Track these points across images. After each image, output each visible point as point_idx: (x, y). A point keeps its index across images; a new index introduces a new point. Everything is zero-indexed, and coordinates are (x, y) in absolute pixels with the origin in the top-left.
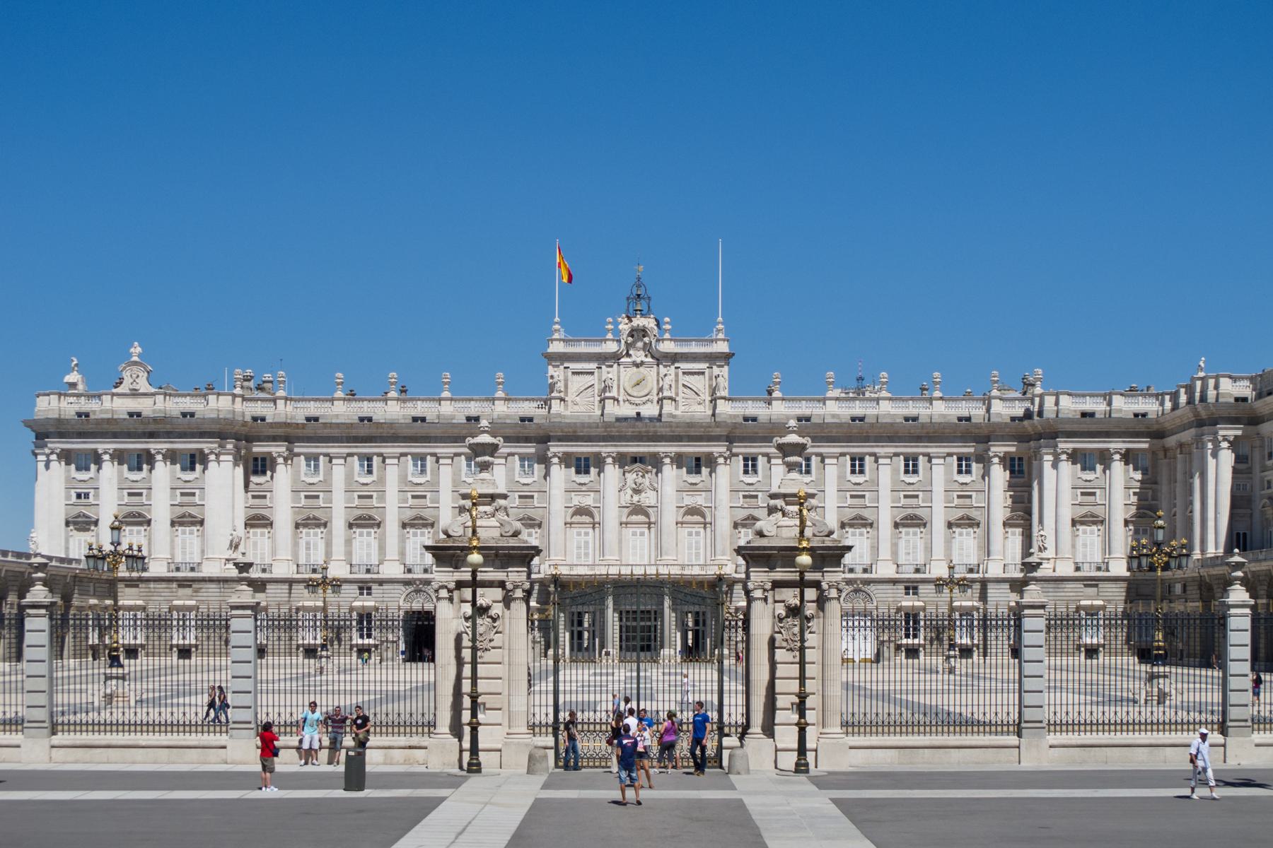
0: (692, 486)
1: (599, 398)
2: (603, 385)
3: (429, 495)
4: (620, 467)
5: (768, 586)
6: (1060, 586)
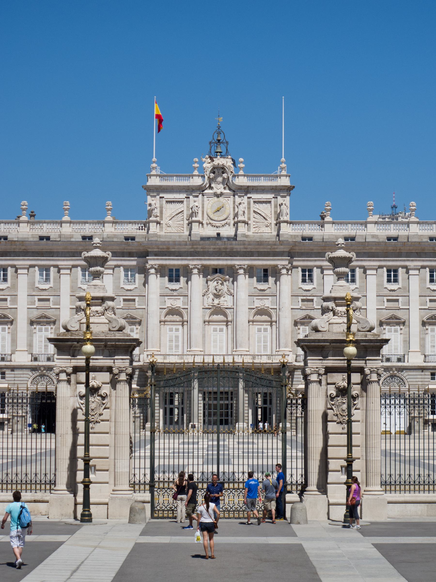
0: (261, 292)
1: (187, 222)
2: (191, 211)
3: (51, 298)
4: (203, 277)
5: (322, 371)
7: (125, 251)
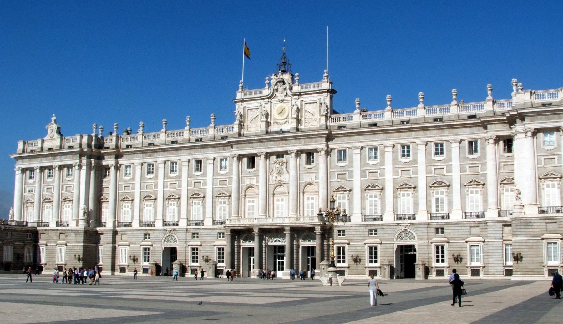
6: (529, 224)
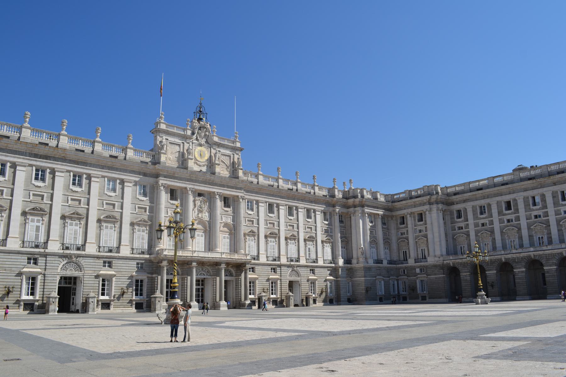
1: (182, 159)
7: (142, 171)
